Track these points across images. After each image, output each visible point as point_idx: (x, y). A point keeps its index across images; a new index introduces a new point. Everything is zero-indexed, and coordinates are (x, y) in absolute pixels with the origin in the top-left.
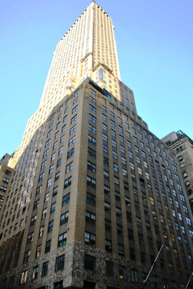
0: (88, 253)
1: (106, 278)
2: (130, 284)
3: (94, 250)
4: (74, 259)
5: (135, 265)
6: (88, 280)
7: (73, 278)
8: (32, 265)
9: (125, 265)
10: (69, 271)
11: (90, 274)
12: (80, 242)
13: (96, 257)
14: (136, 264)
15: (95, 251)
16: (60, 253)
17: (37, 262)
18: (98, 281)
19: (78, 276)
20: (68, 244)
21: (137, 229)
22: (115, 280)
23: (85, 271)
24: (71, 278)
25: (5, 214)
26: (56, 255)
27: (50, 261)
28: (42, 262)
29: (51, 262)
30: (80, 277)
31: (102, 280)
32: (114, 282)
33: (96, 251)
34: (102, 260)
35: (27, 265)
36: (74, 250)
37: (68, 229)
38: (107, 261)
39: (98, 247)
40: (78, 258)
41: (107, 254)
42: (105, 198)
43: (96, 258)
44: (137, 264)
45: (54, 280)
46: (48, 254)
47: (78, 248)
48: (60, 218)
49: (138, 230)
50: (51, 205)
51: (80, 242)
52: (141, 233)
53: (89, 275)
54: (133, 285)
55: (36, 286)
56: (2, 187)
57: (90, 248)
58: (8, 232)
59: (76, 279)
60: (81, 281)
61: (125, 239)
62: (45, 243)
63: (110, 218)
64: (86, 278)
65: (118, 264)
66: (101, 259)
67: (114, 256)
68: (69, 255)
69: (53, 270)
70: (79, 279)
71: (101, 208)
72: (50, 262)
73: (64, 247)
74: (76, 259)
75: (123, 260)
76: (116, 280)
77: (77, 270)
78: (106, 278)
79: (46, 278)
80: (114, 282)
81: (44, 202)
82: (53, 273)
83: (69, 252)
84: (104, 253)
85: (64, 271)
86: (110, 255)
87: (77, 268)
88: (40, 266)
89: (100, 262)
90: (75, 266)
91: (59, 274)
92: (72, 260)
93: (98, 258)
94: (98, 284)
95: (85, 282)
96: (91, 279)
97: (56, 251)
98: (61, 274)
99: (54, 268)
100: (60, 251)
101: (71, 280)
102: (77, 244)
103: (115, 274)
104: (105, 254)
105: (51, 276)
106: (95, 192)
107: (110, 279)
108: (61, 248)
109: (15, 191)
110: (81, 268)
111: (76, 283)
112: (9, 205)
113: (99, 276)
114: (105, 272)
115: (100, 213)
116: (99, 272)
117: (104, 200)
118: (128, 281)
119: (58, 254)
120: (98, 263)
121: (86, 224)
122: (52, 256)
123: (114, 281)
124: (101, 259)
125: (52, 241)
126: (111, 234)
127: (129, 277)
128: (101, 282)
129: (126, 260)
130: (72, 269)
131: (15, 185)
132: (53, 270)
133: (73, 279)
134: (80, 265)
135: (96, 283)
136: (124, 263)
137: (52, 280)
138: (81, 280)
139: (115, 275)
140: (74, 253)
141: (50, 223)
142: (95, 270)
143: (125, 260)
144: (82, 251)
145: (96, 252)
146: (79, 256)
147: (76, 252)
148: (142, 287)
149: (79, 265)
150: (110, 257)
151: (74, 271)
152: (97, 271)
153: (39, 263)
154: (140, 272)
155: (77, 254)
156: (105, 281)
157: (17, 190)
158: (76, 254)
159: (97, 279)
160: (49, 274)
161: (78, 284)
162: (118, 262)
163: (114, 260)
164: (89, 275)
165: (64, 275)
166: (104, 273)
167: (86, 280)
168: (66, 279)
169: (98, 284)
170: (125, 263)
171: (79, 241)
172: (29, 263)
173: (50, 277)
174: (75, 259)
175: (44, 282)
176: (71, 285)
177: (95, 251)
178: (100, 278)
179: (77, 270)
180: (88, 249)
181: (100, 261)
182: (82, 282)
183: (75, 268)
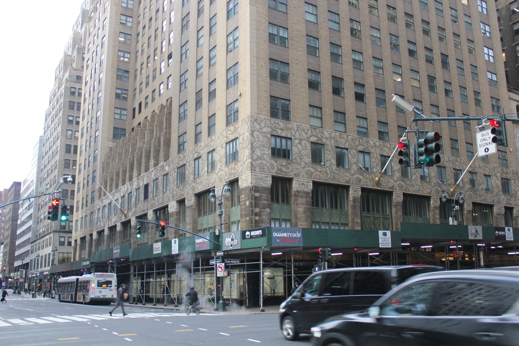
0: (277, 132)
2: (355, 176)
3: (288, 126)
4: (252, 144)
5: (365, 145)
8: (191, 156)
9: (347, 146)
10: (246, 163)
12: (262, 117)
13: (293, 138)
14: (367, 142)
15: (290, 127)
16: (230, 136)
17: (199, 150)
18: (297, 175)
19: (262, 169)
20: (242, 120)
21: (373, 81)
22: (328, 171)
24: (250, 174)
25: (139, 68)
26: (225, 139)
27: (219, 148)
28: (206, 150)
29: (219, 150)
31: (303, 173)
32: (325, 174)
34: (303, 142)
35: (185, 157)
36: (252, 131)
37: (240, 96)
38: (312, 142)
39: (295, 121)
41: (313, 130)
42: (306, 29)
43: (291, 139)
44: (371, 142)
45: (226, 178)
46: (213, 138)
47: (258, 127)
48: (225, 75)
49: (375, 83)
50: (208, 52)
51: (262, 117)
52: (381, 88)
53: (280, 167)
54: (361, 177)
55: (201, 187)
56: (122, 16)
57: (281, 124)
58: (149, 100)
59: (259, 175)
61: (347, 101)
62: (207, 118)
63: (319, 66)
64: (276, 173)
65: (333, 145)
66: (301, 140)
67: (325, 133)
68: (245, 138)
69: (223, 162)
71: (299, 51)
72: (217, 150)
73: (237, 126)
76: (331, 172)
77: (260, 162)
78: (311, 169)
79: (214, 174)
80: (325, 174)
81: (196, 47)
82: (223, 168)
83: (244, 134)
85: (239, 164)
88: (204, 157)
89: (299, 146)
90: (255, 155)
91: (232, 169)
92: (250, 147)
93: (296, 139)
95: (274, 178)
96: (285, 172)
97: (225, 133)
98: (235, 169)
99: (224, 160)
100: (230, 132)
101: (250, 176)
102: (256, 120)
103: (328, 162)
104: (309, 132)
105: (221, 172)
106: (287, 20)
107: (319, 170)
108: (232, 128)
109: (148, 21)
110: (265, 157)
111: (259, 181)
112: (143, 51)
113: (299, 167)
114: (310, 160)
115: (297, 60)
116: (298, 160)
117: (304, 34)
118: (353, 171)
119: (229, 138)
121: (271, 84)
122: (219, 141)
124: (301, 140)
125: (217, 116)
126: (321, 95)
127: (354, 165)
128: (303, 175)
129: (350, 137)
130: (250, 160)
131: (146, 10)
132: (223, 162)
133: (253, 176)
135: (293, 178)
137: (223, 177)
139: (328, 164)
140: (252, 135)
141: (210, 84)
142: (291, 159)
143: (348, 137)
144: (265, 130)
145: (292, 128)
146: (261, 138)
147: (255, 133)
148: (377, 179)
150: (319, 136)
151: (254, 163)
152: (295, 159)
153: (201, 151)
154: (375, 156)
155: (258, 137)
157: (151, 19)
158: (255, 136)
160: (218, 170)
161: (261, 182)
162: (333, 141)
164: (280, 167)
165: (240, 170)
168: (243, 176)
170: (347, 143)
171: (259, 114)
172: (187, 154)
173: (219, 174)
175: (213, 181)
176: (250, 185)
177: (290, 127)
178: (301, 170)
179: (260, 162)
180: (277, 126)
181: (300, 143)
183: (255, 157)
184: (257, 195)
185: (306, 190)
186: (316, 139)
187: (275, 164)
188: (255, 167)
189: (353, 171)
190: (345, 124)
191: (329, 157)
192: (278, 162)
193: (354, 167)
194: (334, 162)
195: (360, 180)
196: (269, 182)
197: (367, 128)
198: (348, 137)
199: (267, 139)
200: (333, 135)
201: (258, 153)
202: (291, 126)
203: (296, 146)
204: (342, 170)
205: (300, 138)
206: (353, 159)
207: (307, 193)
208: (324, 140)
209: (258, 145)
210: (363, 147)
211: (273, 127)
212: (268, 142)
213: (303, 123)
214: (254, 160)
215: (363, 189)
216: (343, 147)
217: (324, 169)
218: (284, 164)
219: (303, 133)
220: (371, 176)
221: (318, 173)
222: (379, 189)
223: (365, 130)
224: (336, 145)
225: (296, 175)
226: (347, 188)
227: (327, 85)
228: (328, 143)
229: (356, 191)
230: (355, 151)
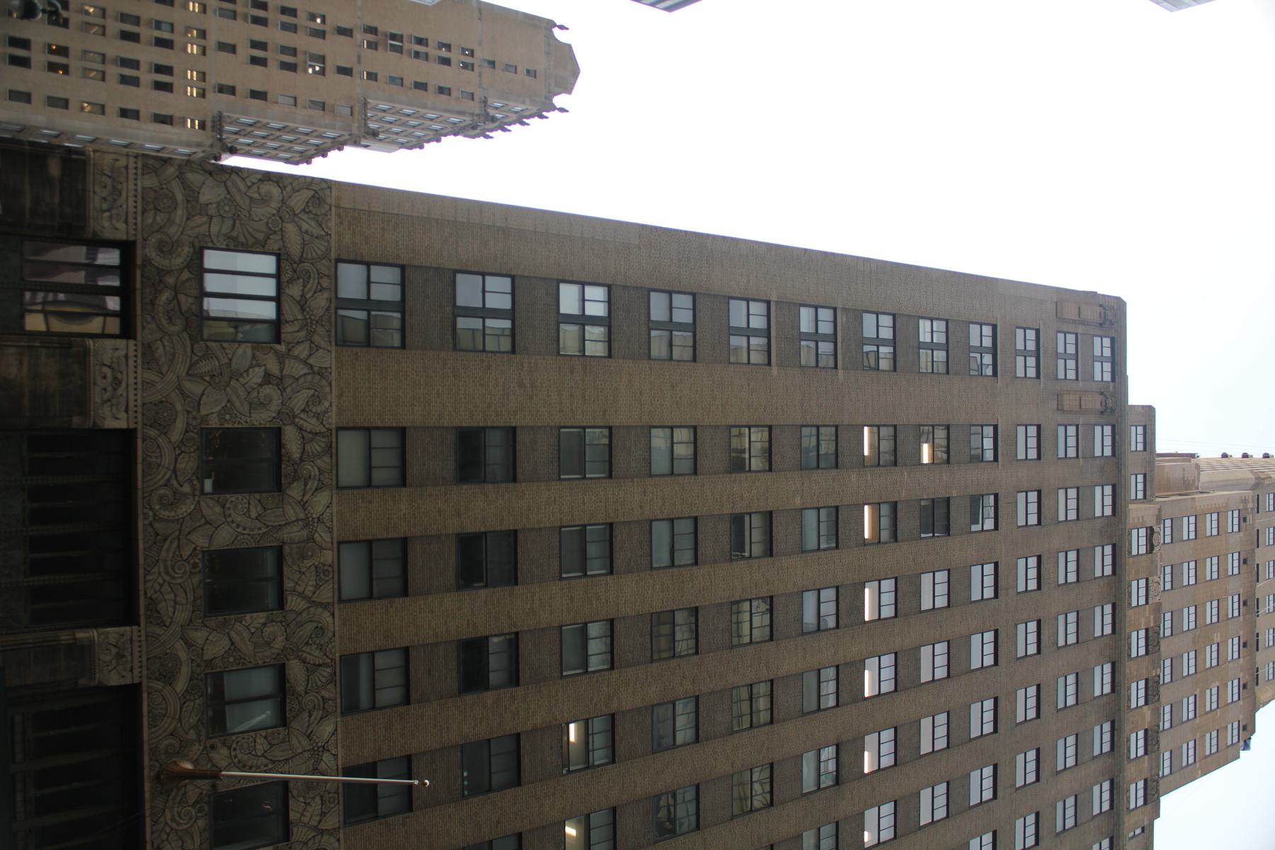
0: (290, 281)
1: (180, 423)
3: (320, 330)
6: (138, 273)
7: (132, 160)
9: (293, 602)
11: (176, 291)
19: (154, 201)
22: (184, 509)
30: (144, 211)
33: (318, 348)
40: (247, 201)
43: (279, 343)
47: (298, 201)
59: (131, 186)
60: (126, 222)
64: (147, 261)
65: (286, 534)
67: (322, 499)
70: (131, 203)
74: (239, 190)
75: (317, 587)
78: (180, 423)
84: (320, 409)
86: (319, 462)
87: (192, 195)
89: (256, 375)
93: (281, 358)
94: (132, 353)
96: (153, 303)
103: (218, 509)
110: (198, 220)
111: (109, 182)
114: (214, 422)
116: (205, 367)
120: (254, 357)
123: (178, 498)
127: (226, 643)
133: (123, 162)
134: (211, 217)
136: (301, 595)
138: (131, 220)
139: (211, 509)
143: (325, 606)
146: (261, 212)
147: (275, 191)
149: (212, 211)
151: (171, 170)
156: (158, 416)
159: (160, 350)
161: (105, 193)
163: (304, 505)
164: (170, 280)
166: (203, 412)
167: (139, 262)
169: (132, 353)
171: (339, 216)
174: (234, 177)
179: (179, 197)
180: (312, 284)
182: (121, 226)
184: (54, 168)
185: (96, 396)
186: (296, 456)
187: (178, 261)
188: (155, 171)
189: (199, 636)
190: (370, 597)
191: (236, 522)
192: (186, 275)
193: (216, 646)
194: (224, 538)
195: (168, 677)
196: (107, 224)
197: (373, 707)
198: (325, 606)
199: (261, 236)
200: (322, 535)
201: (210, 193)
202: (323, 344)
203: (255, 362)
204: (196, 579)
205: (288, 381)
206: (246, 634)
207: (81, 402)
208: (295, 491)
209: (238, 198)
210: (301, 689)
211: (306, 266)
212: (251, 241)
213: (340, 396)
214: (181, 176)
215: (131, 693)
216: (288, 585)
217: (187, 488)
218: (182, 298)
219: (304, 395)
220: (192, 734)
221: (167, 460)
222: (147, 786)
223: (364, 699)
224: (286, 549)
225: (148, 349)
226: (130, 618)
227: (483, 508)
228: (292, 512)
229: (120, 656)
230: (279, 644)
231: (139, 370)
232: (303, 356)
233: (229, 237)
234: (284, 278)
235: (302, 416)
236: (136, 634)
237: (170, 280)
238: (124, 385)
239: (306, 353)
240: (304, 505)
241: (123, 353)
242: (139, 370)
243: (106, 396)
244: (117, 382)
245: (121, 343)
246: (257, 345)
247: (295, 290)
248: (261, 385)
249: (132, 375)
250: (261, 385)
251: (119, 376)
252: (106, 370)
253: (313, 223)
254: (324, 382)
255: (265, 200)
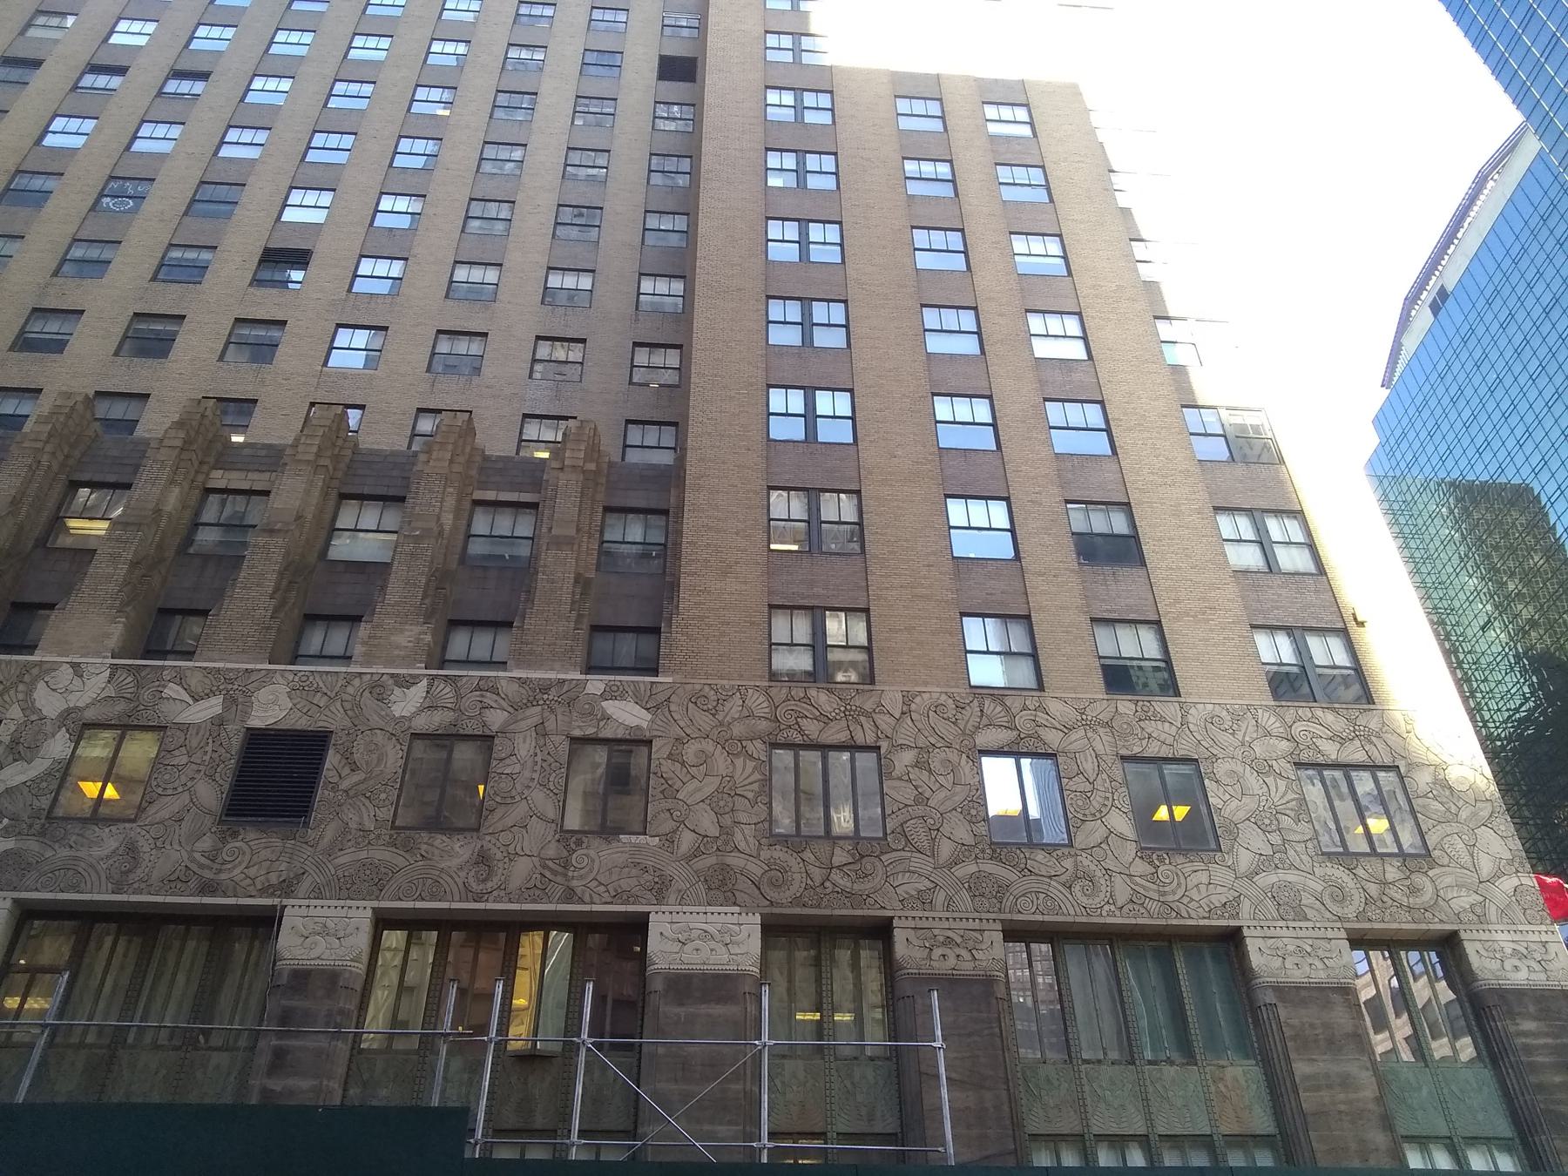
0: (801, 731)
13: (884, 745)
23: (776, 854)
67: (1054, 707)
78: (990, 867)
163: (1068, 729)
187: (793, 861)
192: (807, 855)
205: (921, 742)
208: (1053, 738)
209: (708, 790)
212: (757, 776)
218: (837, 861)
231: (927, 914)
232: (892, 721)
233: (753, 804)
234: (799, 740)
235: (961, 724)
236: (1258, 932)
237: (817, 874)
238: (950, 934)
239: (886, 718)
240: (1068, 729)
241: (911, 934)
242: (927, 914)
243: (964, 953)
244: (949, 942)
245: (899, 936)
246: (882, 773)
247: (812, 728)
248: (930, 771)
249: (937, 924)
250: (930, 771)
251: (941, 939)
252: (937, 952)
253: (728, 705)
254: (918, 700)
255: (705, 758)
